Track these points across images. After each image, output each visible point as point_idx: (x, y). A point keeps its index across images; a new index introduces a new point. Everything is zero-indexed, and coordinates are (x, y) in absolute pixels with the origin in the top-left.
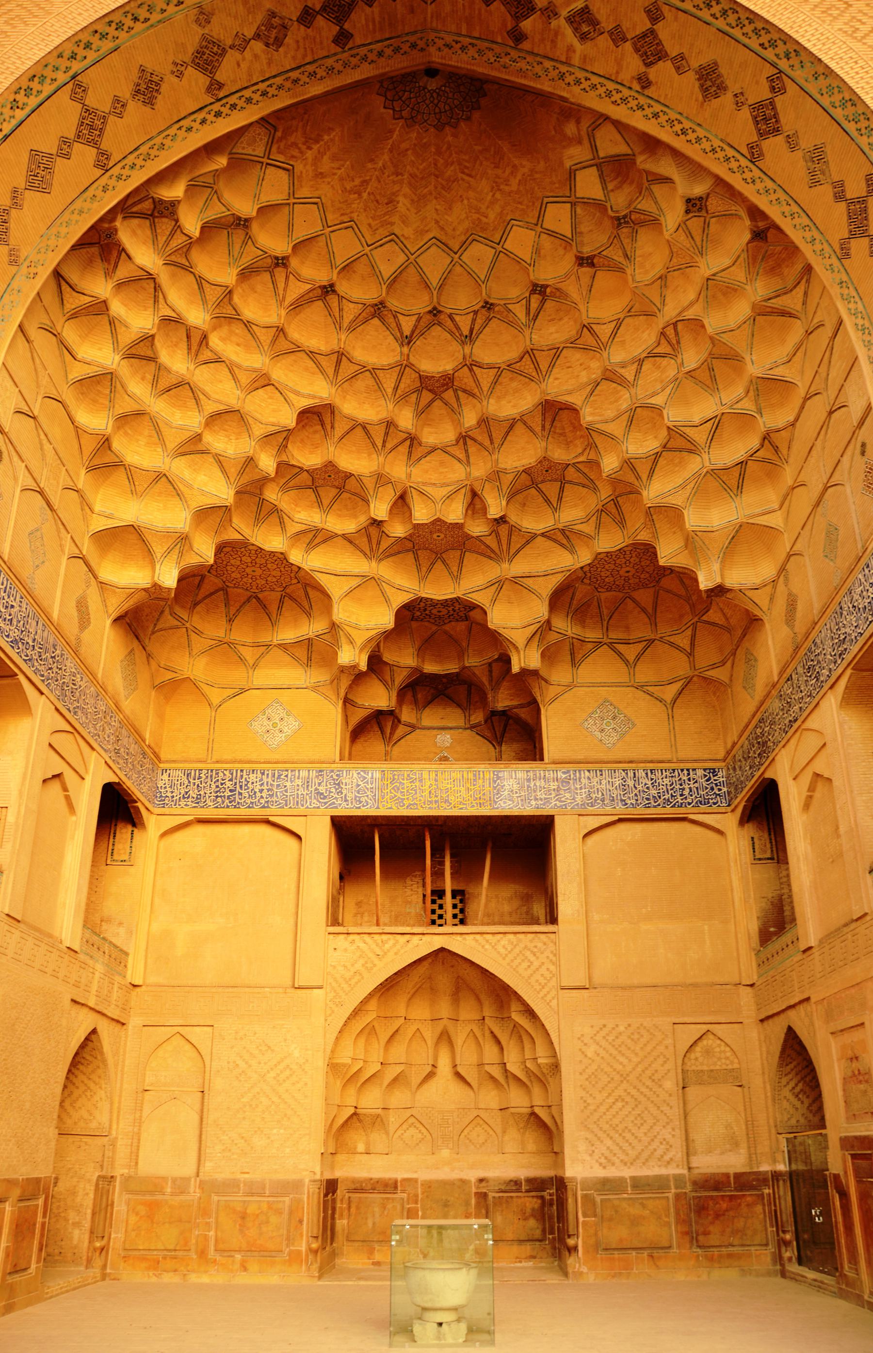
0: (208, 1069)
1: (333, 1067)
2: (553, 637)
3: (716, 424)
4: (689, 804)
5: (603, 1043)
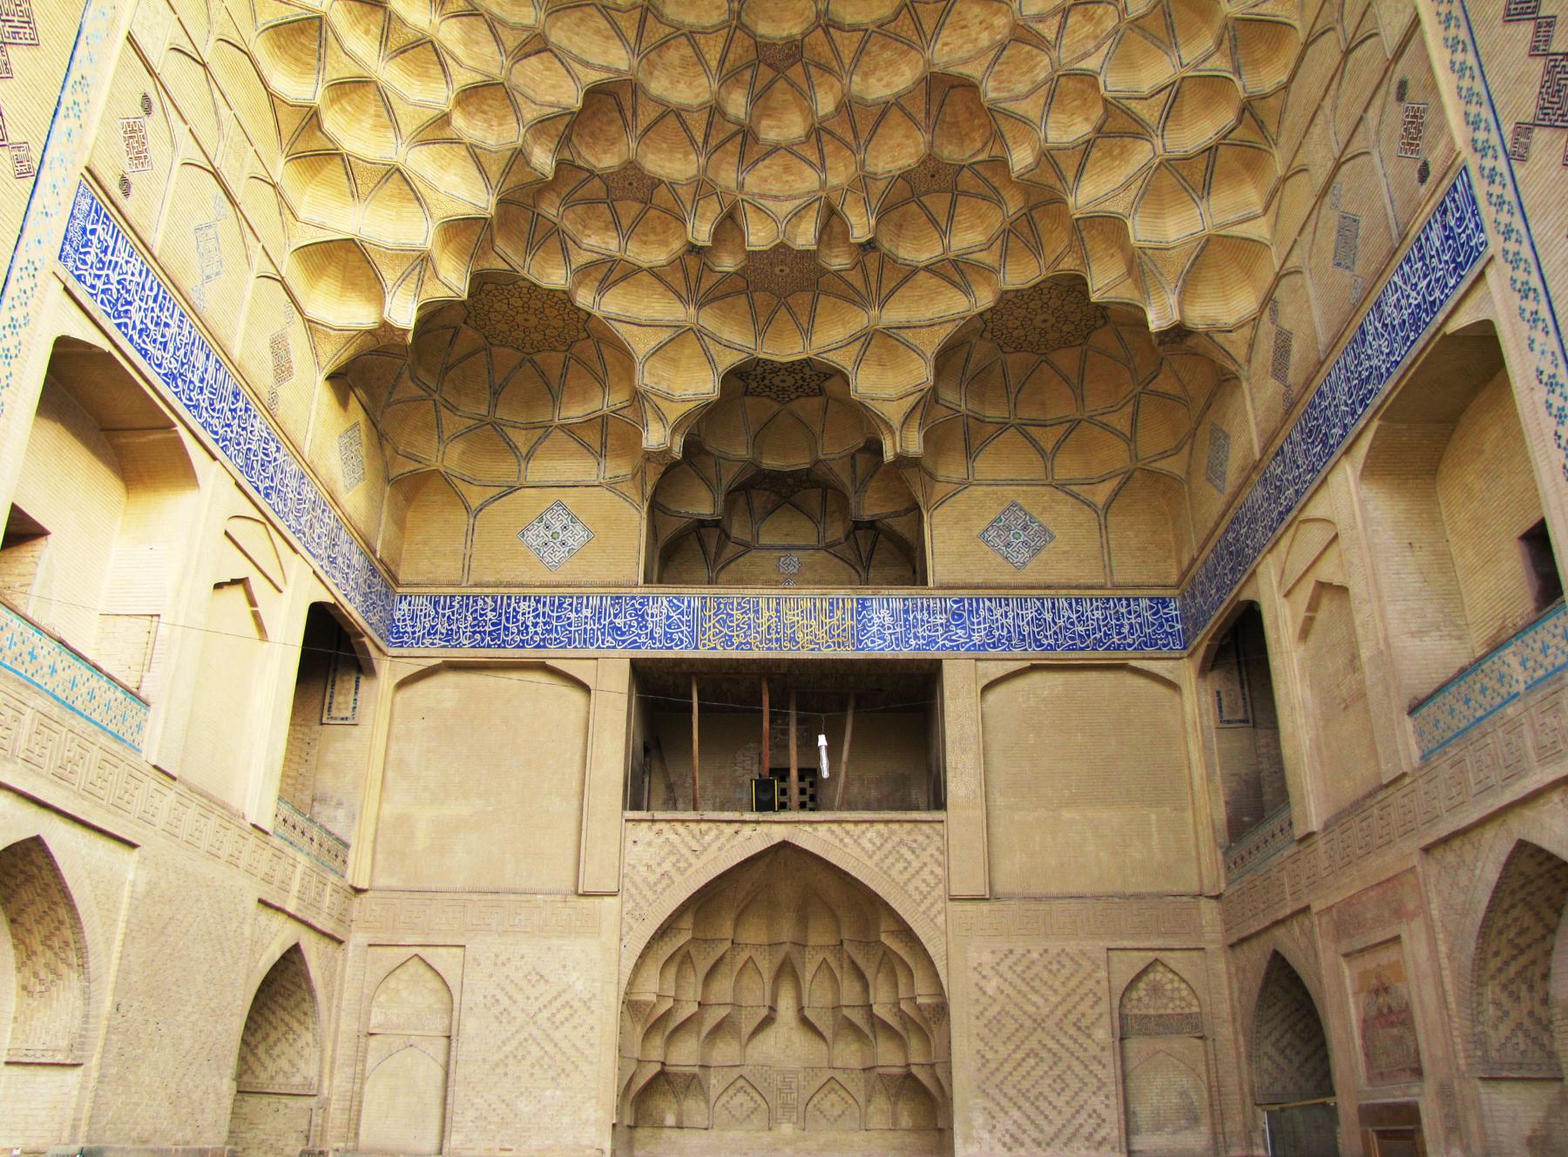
0: (456, 1006)
1: (631, 1006)
2: (940, 413)
3: (1174, 96)
4: (1130, 645)
5: (1009, 975)
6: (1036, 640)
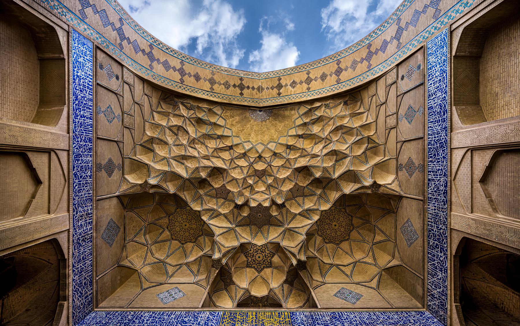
3: (351, 148)
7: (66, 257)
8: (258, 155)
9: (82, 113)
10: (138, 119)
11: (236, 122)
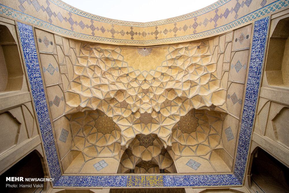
3: (200, 79)
6: (205, 184)
7: (43, 156)
8: (144, 79)
9: (34, 76)
10: (69, 65)
11: (130, 57)
